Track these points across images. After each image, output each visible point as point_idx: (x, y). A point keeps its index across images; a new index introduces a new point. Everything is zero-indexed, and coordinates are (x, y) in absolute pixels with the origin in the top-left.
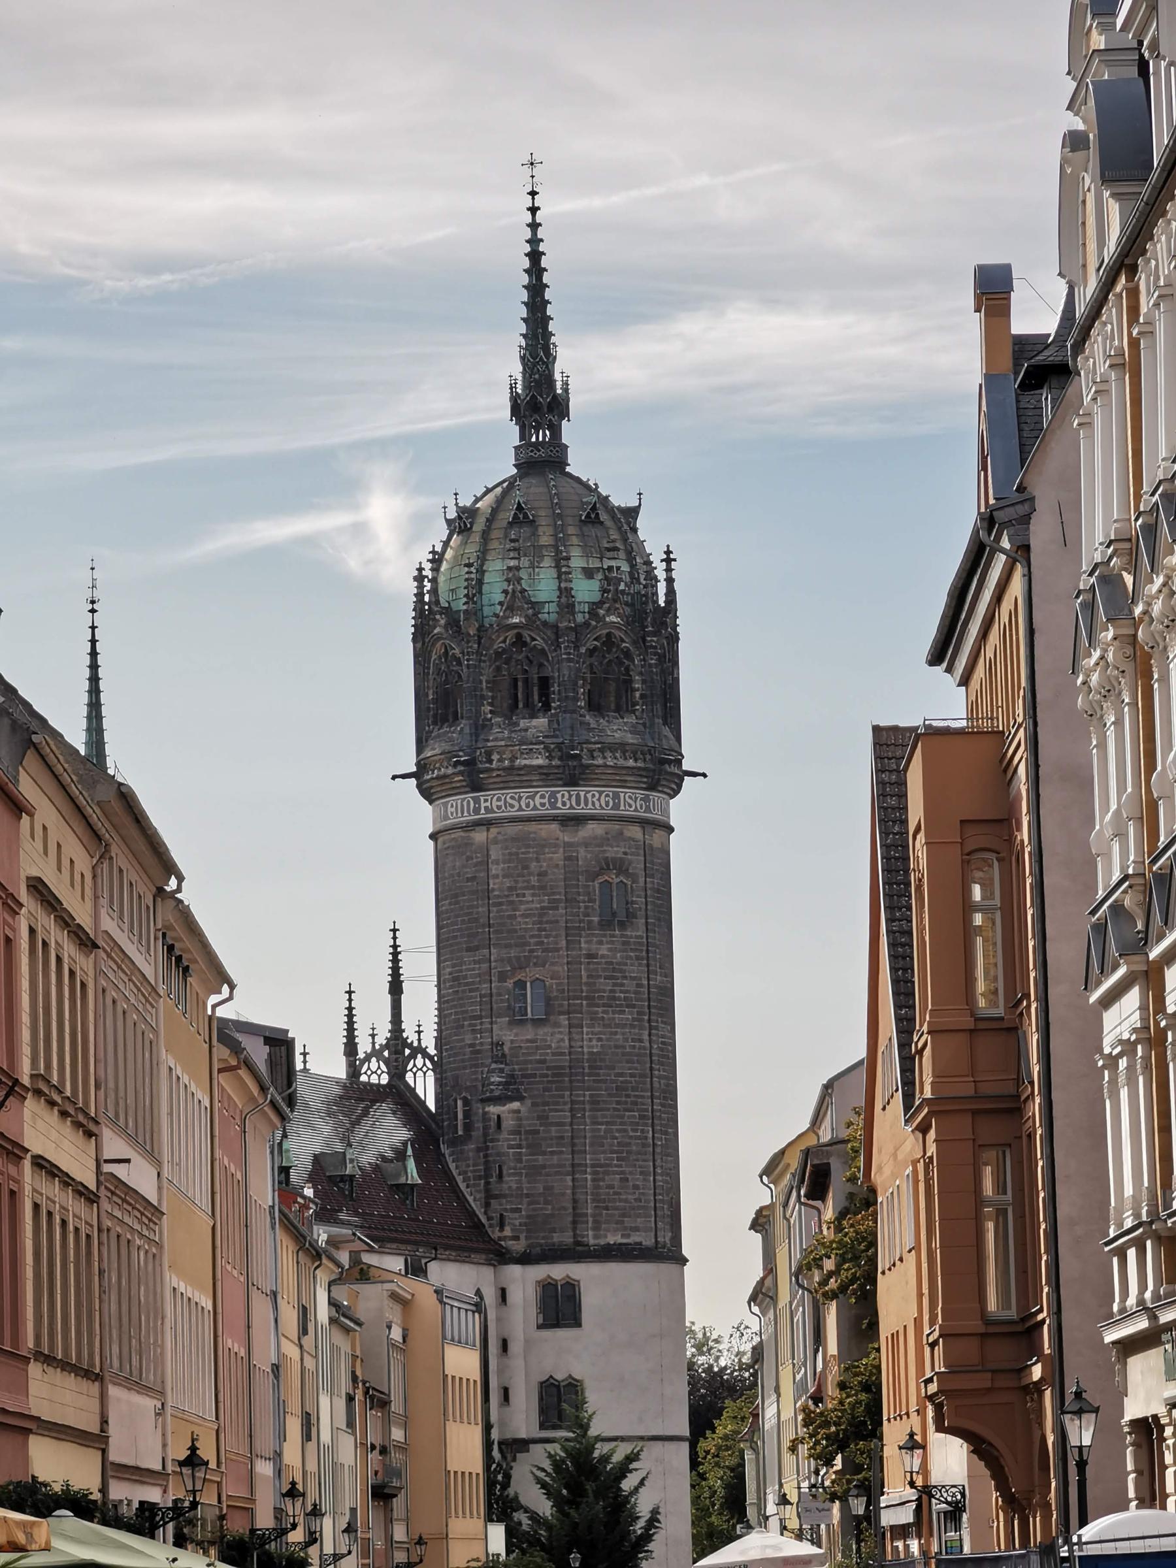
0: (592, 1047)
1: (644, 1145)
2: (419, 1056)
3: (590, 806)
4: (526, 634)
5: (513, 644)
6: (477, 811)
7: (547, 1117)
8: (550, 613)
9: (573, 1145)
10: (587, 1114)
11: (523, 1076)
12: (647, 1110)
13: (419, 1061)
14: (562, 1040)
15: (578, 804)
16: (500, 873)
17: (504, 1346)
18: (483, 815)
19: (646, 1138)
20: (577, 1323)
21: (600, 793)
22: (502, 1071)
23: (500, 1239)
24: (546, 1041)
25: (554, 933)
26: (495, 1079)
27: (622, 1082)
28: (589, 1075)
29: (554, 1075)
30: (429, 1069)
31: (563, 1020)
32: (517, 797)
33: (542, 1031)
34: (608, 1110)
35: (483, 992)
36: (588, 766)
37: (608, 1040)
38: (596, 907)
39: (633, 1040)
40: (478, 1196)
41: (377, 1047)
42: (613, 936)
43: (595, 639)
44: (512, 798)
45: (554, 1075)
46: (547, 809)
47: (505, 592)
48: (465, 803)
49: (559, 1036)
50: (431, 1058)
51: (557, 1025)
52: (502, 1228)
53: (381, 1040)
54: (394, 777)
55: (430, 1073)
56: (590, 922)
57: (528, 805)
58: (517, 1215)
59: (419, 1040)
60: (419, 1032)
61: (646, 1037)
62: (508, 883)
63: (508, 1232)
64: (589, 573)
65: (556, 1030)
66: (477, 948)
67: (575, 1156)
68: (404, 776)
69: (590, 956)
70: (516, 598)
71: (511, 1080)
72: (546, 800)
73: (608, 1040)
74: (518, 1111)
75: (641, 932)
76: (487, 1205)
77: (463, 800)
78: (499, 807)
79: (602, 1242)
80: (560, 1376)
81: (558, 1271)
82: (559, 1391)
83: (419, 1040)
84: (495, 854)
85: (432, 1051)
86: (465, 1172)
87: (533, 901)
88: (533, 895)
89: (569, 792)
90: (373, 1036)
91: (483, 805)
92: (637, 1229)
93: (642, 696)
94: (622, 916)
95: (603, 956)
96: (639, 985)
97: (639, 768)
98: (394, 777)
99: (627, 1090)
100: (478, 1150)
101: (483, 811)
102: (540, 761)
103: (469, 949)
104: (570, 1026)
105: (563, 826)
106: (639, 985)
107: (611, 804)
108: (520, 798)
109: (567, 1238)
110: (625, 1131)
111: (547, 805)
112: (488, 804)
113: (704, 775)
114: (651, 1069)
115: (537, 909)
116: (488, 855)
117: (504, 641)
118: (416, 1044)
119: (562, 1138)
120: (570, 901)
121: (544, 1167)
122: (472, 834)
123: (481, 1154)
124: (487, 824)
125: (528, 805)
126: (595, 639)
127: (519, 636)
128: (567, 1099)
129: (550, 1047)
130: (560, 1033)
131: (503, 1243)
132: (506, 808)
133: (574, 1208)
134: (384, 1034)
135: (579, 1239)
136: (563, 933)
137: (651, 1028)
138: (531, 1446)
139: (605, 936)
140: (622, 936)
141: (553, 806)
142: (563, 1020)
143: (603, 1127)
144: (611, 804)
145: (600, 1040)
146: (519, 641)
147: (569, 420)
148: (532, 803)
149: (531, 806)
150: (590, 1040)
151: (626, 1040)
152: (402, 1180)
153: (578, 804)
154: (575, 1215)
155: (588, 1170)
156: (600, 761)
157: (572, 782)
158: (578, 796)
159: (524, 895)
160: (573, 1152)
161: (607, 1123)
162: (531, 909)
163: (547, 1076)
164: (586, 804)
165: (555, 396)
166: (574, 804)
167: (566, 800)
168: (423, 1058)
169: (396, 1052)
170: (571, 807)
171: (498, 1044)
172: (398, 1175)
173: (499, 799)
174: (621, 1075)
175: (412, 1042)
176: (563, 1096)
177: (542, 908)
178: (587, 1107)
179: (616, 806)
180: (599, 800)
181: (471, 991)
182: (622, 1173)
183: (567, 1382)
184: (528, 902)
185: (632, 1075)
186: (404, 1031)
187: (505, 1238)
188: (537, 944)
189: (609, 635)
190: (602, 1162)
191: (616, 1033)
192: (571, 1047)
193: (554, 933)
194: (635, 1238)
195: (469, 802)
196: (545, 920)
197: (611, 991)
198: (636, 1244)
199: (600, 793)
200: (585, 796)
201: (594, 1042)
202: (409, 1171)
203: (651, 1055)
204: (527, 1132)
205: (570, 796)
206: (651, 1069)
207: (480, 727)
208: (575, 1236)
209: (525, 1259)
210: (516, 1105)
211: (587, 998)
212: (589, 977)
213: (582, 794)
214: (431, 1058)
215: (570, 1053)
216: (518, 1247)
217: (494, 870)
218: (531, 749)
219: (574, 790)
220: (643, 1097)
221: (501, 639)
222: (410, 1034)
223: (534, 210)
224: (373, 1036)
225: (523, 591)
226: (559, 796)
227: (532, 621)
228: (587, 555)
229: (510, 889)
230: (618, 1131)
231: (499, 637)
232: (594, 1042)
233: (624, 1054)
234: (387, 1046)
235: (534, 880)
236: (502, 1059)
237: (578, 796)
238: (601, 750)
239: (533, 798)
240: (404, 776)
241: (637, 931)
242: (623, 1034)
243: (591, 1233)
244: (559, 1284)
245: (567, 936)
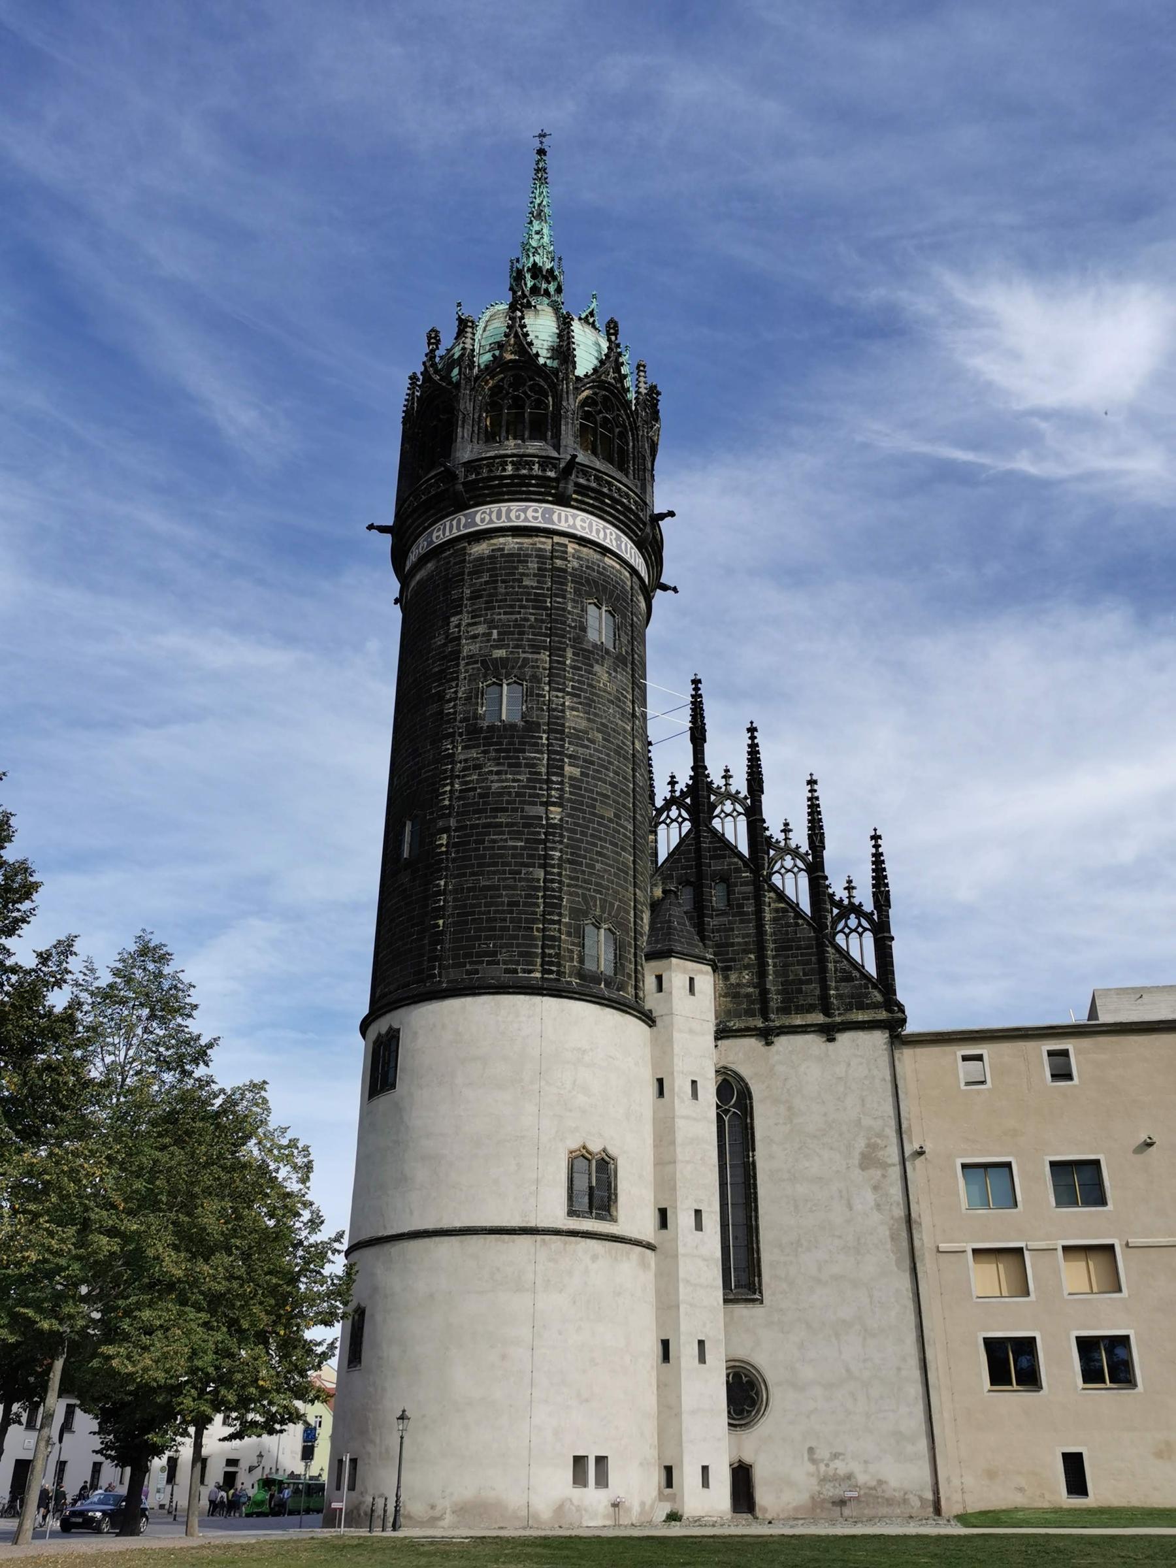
46: (540, 522)
54: (371, 527)
57: (518, 517)
68: (383, 529)
72: (539, 514)
98: (371, 527)
111: (540, 519)
113: (675, 590)
125: (518, 517)
148: (522, 516)
239: (525, 510)
240: (383, 529)
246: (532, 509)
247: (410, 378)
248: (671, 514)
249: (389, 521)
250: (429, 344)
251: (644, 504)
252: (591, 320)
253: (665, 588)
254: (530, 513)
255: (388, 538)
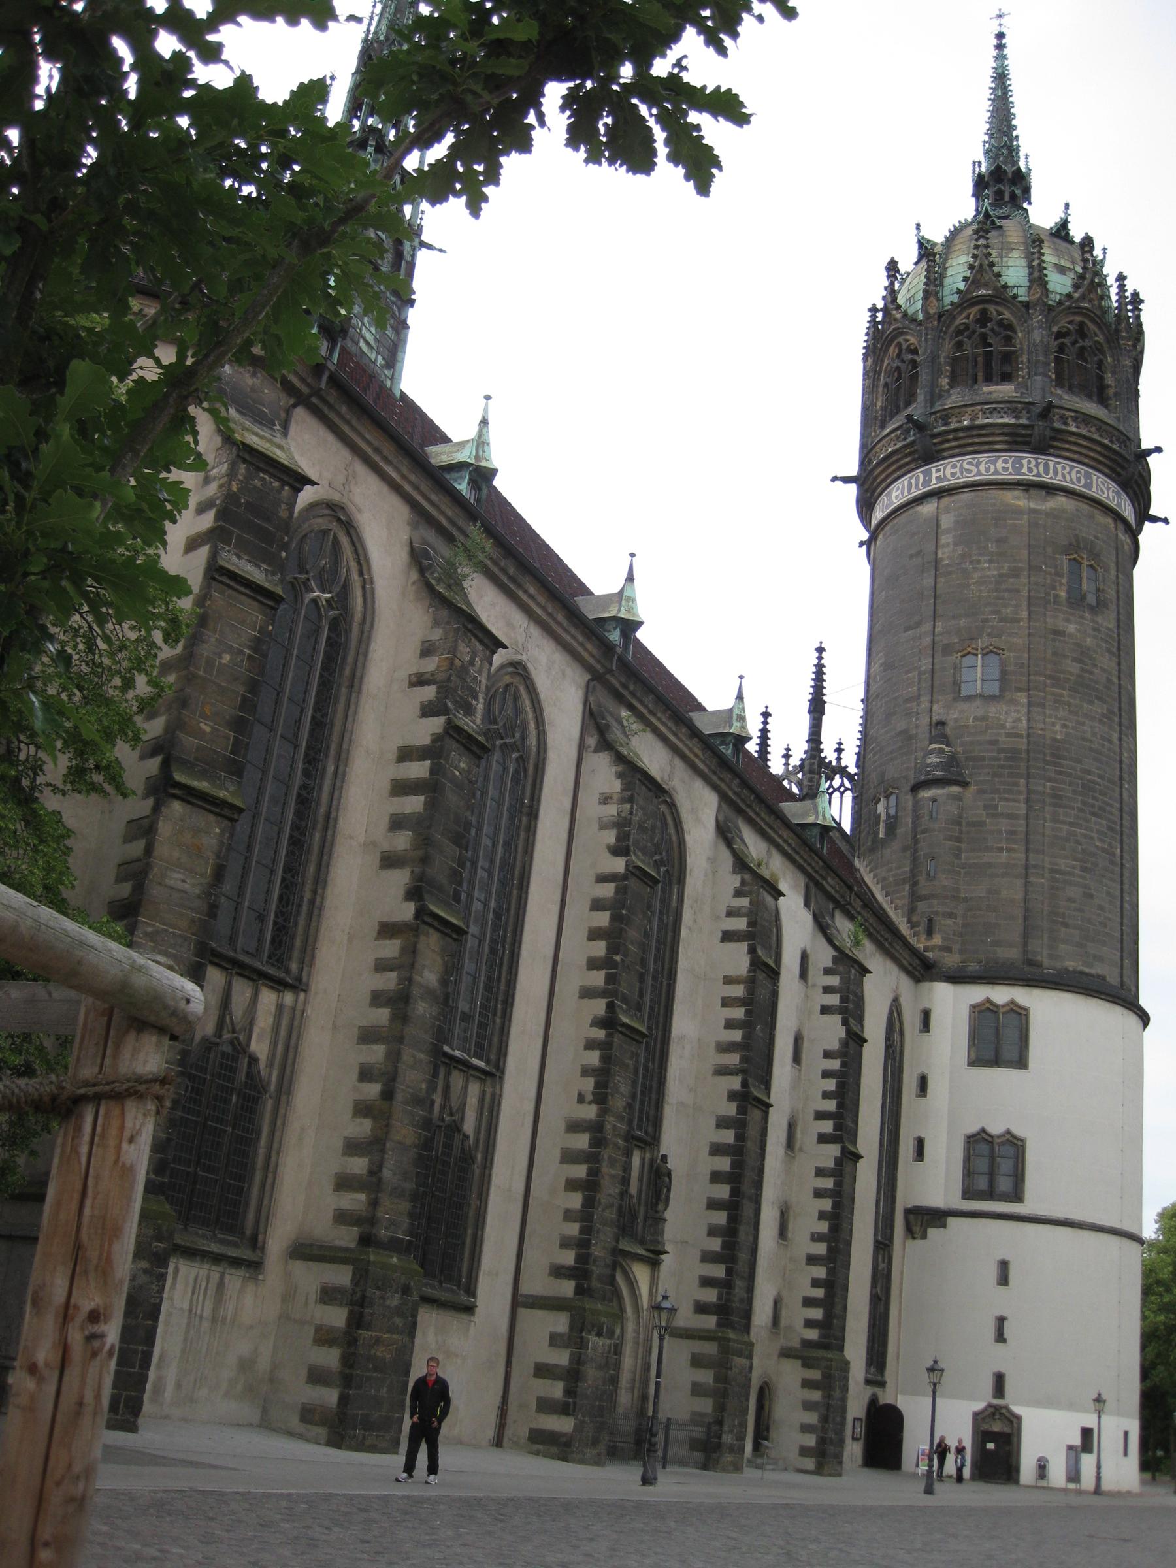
0: (1056, 733)
1: (1112, 863)
2: (837, 776)
3: (1059, 477)
4: (992, 309)
5: (977, 321)
6: (927, 482)
7: (996, 807)
8: (1023, 294)
9: (1027, 842)
10: (1047, 808)
11: (967, 759)
12: (1114, 822)
13: (837, 782)
14: (1019, 720)
15: (1046, 472)
16: (950, 540)
17: (923, 1084)
18: (934, 485)
19: (1114, 855)
20: (1021, 1062)
21: (1072, 468)
22: (941, 751)
23: (926, 949)
24: (999, 719)
25: (1014, 603)
26: (933, 759)
27: (1089, 781)
28: (1055, 764)
29: (1007, 759)
30: (847, 789)
31: (1022, 698)
32: (975, 462)
33: (993, 710)
34: (1073, 808)
35: (923, 668)
36: (1060, 431)
37: (1073, 728)
38: (1064, 581)
39: (1103, 738)
40: (900, 902)
41: (790, 768)
42: (1082, 617)
43: (1070, 322)
44: (970, 463)
45: (1007, 759)
47: (971, 267)
48: (913, 481)
49: (1014, 715)
50: (851, 777)
51: (1013, 702)
52: (930, 933)
53: (795, 761)
54: (834, 479)
55: (848, 795)
56: (1056, 596)
57: (988, 470)
58: (949, 922)
59: (839, 759)
60: (839, 751)
61: (1116, 736)
62: (959, 550)
63: (937, 940)
64: (1062, 270)
65: (1013, 708)
66: (918, 624)
67: (1031, 855)
68: (847, 480)
69: (1057, 633)
70: (982, 271)
71: (952, 761)
72: (1009, 465)
73: (1073, 728)
74: (959, 798)
75: (1112, 625)
76: (912, 910)
77: (911, 478)
78: (953, 475)
79: (1058, 965)
80: (996, 1129)
81: (1001, 995)
82: (992, 1150)
83: (839, 759)
84: (946, 521)
85: (852, 770)
86: (884, 879)
87: (989, 568)
88: (990, 562)
89: (1036, 459)
90: (787, 756)
91: (935, 475)
92: (1100, 959)
93: (1116, 394)
94: (1091, 599)
95: (1070, 635)
96: (1109, 680)
97: (1114, 451)
98: (834, 479)
99: (1095, 791)
100: (905, 849)
101: (934, 481)
102: (1005, 420)
103: (907, 629)
104: (1030, 704)
105: (1027, 490)
106: (1109, 680)
107: (1083, 481)
108: (979, 463)
109: (1011, 954)
110: (1092, 838)
112: (941, 473)
113: (1166, 521)
114: (1121, 778)
115: (994, 576)
116: (938, 525)
117: (967, 317)
118: (834, 763)
119: (1013, 833)
120: (1033, 568)
121: (990, 865)
122: (919, 508)
123: (908, 854)
124: (938, 494)
125: (988, 470)
126: (1070, 322)
127: (984, 312)
128: (1023, 788)
129: (1003, 727)
130: (1017, 711)
131: (929, 954)
132: (962, 473)
133: (1026, 918)
134: (799, 753)
135: (1030, 957)
136: (1025, 604)
137: (1120, 733)
138: (951, 1221)
139: (1073, 615)
140: (1093, 621)
141: (1018, 471)
142: (1022, 698)
143: (1065, 827)
144: (1083, 481)
145: (1064, 726)
146: (984, 318)
147: (1030, 203)
148: (992, 469)
149: (992, 469)
150: (1054, 724)
151: (1094, 734)
152: (811, 819)
153: (1046, 472)
154: (1026, 928)
155: (1047, 875)
156: (1073, 429)
157: (1041, 448)
158: (1046, 466)
159: (979, 562)
160: (1027, 850)
161: (1071, 824)
162: (988, 576)
163: (998, 759)
164: (1056, 473)
165: (1019, 169)
166: (1042, 472)
167: (1030, 466)
168: (841, 778)
169: (811, 772)
170: (1038, 475)
171: (937, 724)
172: (806, 814)
173: (954, 467)
174: (1089, 772)
175: (830, 762)
176: (1016, 784)
177: (1001, 576)
178: (1048, 800)
179: (1088, 485)
180: (1069, 473)
181: (907, 672)
182: (1086, 886)
183: (1004, 1139)
184: (984, 569)
185: (1100, 777)
186: (822, 751)
187: (933, 948)
188: (993, 612)
189: (1082, 324)
190: (1063, 867)
191: (1083, 724)
192: (1029, 728)
193: (1014, 603)
194: (1098, 969)
195: (918, 478)
196: (1003, 587)
197: (1079, 676)
198: (1099, 976)
199: (1072, 468)
200: (1054, 467)
201: (1058, 728)
202: (820, 809)
203: (1121, 762)
204: (969, 824)
205: (1037, 465)
206: (1121, 778)
207: (934, 396)
208: (1025, 952)
209: (957, 978)
210: (956, 789)
211: (1051, 677)
212: (1055, 654)
213: (1051, 464)
214: (851, 777)
215: (1028, 735)
216: (951, 960)
217: (944, 539)
218: (995, 409)
219: (1042, 459)
220: (1111, 806)
221: (964, 315)
222: (829, 754)
223: (1000, 47)
224: (787, 756)
225: (992, 265)
226: (1025, 462)
227: (1002, 295)
228: (1057, 252)
229: (963, 556)
230: (1085, 836)
231: (960, 313)
232: (1058, 728)
233: (1091, 749)
234: (801, 767)
235: (992, 547)
236: (944, 738)
237: (1046, 466)
238: (1075, 419)
239: (994, 463)
240: (847, 480)
241: (1107, 621)
242: (1092, 727)
243: (1045, 952)
244: (1002, 1010)
245: (1029, 605)
246: (1000, 460)
247: (870, 310)
248: (1158, 450)
249: (853, 469)
250: (888, 277)
251: (1130, 436)
252: (1063, 233)
253: (1155, 519)
254: (1000, 465)
255: (852, 488)
